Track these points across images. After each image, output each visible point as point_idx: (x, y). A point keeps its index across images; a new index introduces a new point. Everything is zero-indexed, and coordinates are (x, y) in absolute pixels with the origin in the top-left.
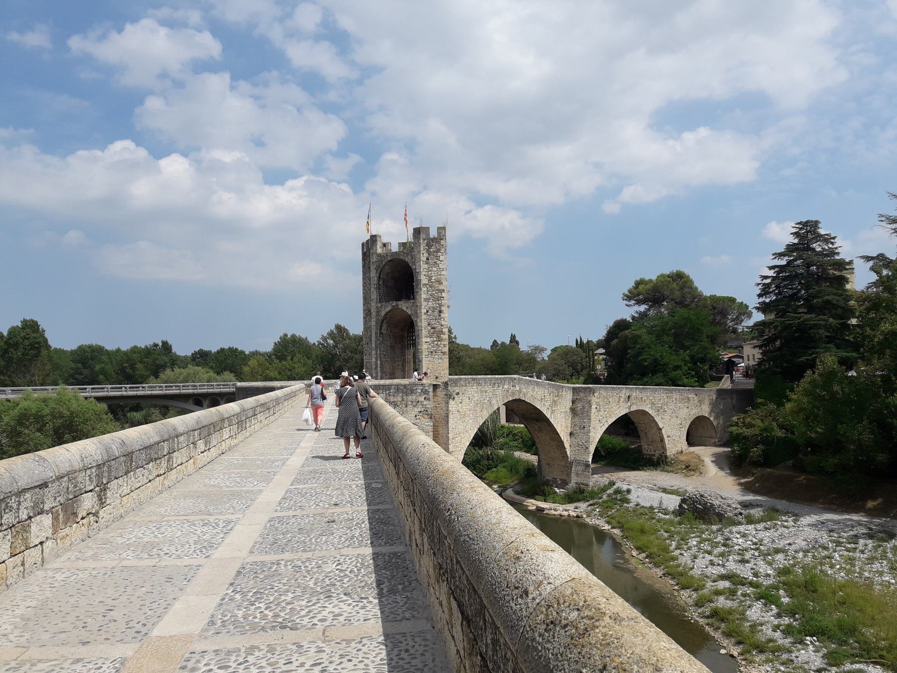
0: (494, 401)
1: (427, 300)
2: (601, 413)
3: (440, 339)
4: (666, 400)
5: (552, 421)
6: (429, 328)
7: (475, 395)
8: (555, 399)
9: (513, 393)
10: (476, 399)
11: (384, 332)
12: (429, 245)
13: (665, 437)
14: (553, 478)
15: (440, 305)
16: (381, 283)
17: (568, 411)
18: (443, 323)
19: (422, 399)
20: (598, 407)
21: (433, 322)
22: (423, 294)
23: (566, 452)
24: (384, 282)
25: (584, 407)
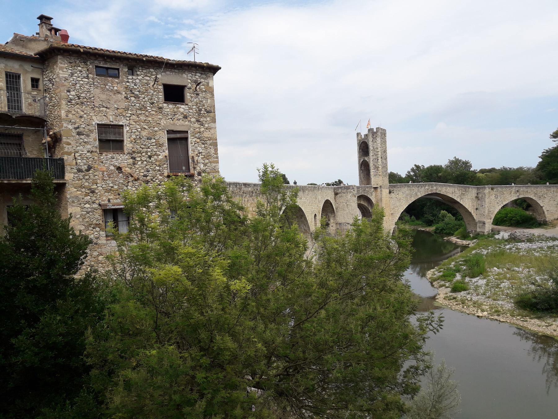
0: (419, 194)
1: (373, 156)
2: (498, 199)
3: (378, 170)
5: (461, 203)
8: (463, 193)
9: (432, 190)
10: (407, 193)
11: (363, 169)
12: (373, 135)
15: (378, 157)
17: (474, 198)
18: (379, 164)
19: (352, 191)
20: (496, 196)
21: (375, 164)
22: (371, 154)
23: (474, 218)
25: (482, 196)
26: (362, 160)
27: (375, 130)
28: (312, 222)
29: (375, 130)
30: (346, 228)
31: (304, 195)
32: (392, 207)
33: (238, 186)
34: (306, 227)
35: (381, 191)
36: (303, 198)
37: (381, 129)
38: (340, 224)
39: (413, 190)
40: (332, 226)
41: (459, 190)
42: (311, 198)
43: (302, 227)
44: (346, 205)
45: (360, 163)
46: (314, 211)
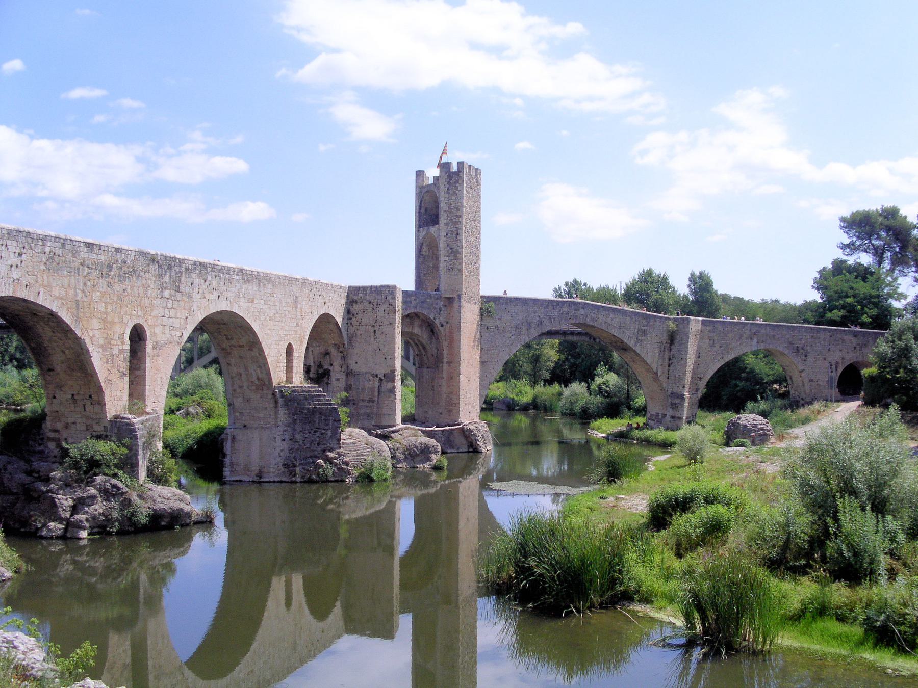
0: (546, 322)
1: (446, 224)
2: (715, 349)
3: (456, 258)
4: (810, 340)
5: (638, 349)
6: (448, 248)
7: (521, 314)
8: (643, 328)
10: (520, 317)
11: (423, 253)
13: (806, 381)
14: (657, 413)
15: (457, 229)
16: (423, 211)
22: (443, 220)
24: (426, 210)
26: (424, 233)
27: (454, 168)
28: (278, 361)
29: (454, 168)
30: (370, 386)
31: (262, 293)
33: (68, 247)
34: (262, 373)
35: (460, 306)
36: (256, 301)
37: (470, 166)
39: (535, 312)
40: (338, 380)
41: (635, 323)
42: (281, 303)
43: (253, 372)
44: (372, 331)
45: (418, 239)
46: (286, 335)
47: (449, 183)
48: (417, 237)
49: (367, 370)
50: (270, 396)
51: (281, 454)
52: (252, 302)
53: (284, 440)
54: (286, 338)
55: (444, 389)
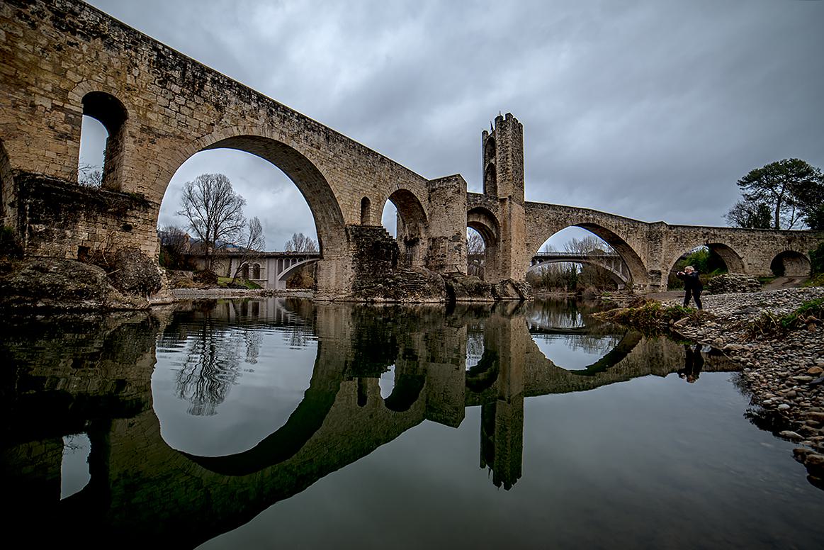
1: (500, 153)
3: (507, 173)
13: (746, 264)
16: (487, 154)
27: (504, 119)
29: (504, 119)
32: (529, 234)
38: (434, 240)
40: (423, 244)
46: (361, 190)
47: (502, 129)
48: (484, 168)
49: (441, 235)
50: (344, 233)
51: (351, 279)
52: (319, 149)
53: (352, 268)
54: (361, 192)
55: (501, 258)
